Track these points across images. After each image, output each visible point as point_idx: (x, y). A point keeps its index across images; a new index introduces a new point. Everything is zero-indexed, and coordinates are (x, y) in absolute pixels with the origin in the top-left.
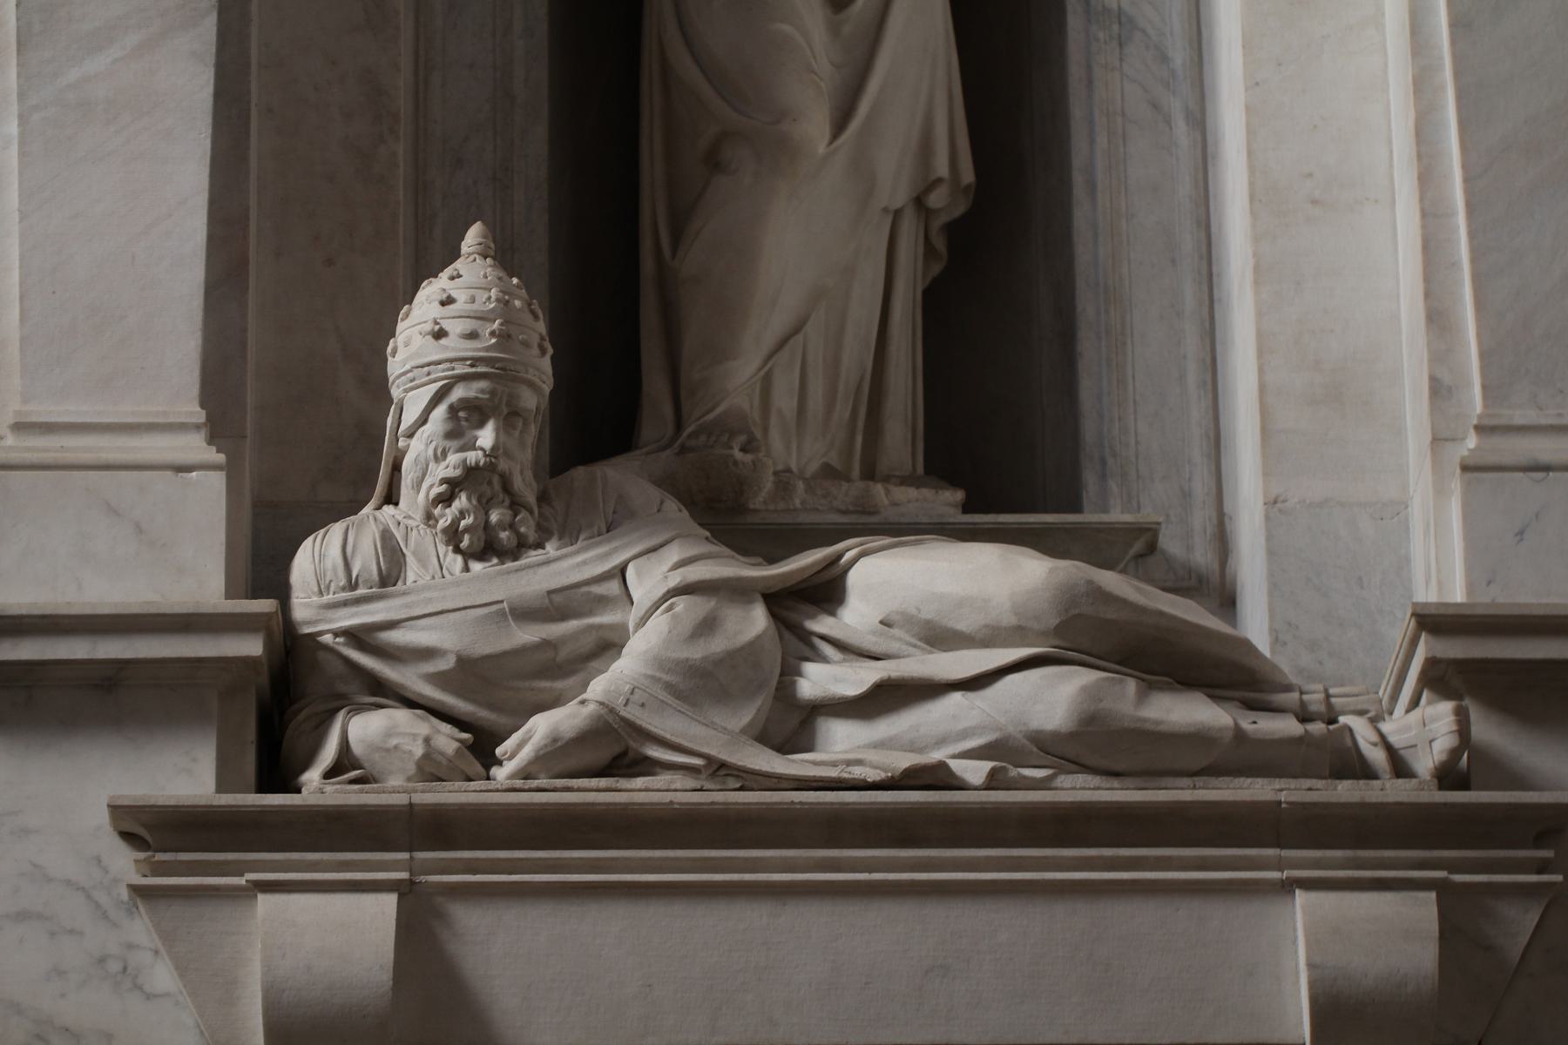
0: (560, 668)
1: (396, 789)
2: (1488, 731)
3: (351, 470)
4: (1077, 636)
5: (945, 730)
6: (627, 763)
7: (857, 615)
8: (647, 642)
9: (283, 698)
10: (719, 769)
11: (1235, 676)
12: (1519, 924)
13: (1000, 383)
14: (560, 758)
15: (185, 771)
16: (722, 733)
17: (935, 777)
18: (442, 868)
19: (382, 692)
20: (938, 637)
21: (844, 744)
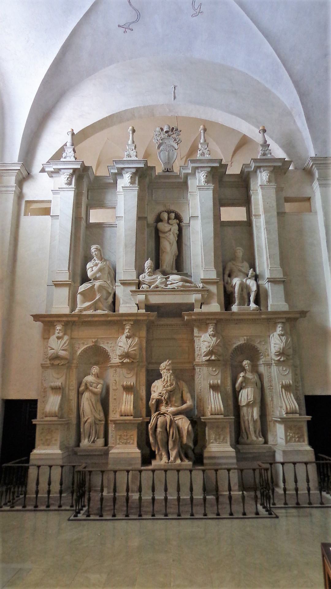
1: (145, 289)
2: (204, 285)
3: (143, 271)
7: (170, 279)
11: (190, 282)
12: (206, 296)
13: (179, 265)
16: (163, 286)
18: (147, 293)
19: (144, 284)
21: (169, 286)
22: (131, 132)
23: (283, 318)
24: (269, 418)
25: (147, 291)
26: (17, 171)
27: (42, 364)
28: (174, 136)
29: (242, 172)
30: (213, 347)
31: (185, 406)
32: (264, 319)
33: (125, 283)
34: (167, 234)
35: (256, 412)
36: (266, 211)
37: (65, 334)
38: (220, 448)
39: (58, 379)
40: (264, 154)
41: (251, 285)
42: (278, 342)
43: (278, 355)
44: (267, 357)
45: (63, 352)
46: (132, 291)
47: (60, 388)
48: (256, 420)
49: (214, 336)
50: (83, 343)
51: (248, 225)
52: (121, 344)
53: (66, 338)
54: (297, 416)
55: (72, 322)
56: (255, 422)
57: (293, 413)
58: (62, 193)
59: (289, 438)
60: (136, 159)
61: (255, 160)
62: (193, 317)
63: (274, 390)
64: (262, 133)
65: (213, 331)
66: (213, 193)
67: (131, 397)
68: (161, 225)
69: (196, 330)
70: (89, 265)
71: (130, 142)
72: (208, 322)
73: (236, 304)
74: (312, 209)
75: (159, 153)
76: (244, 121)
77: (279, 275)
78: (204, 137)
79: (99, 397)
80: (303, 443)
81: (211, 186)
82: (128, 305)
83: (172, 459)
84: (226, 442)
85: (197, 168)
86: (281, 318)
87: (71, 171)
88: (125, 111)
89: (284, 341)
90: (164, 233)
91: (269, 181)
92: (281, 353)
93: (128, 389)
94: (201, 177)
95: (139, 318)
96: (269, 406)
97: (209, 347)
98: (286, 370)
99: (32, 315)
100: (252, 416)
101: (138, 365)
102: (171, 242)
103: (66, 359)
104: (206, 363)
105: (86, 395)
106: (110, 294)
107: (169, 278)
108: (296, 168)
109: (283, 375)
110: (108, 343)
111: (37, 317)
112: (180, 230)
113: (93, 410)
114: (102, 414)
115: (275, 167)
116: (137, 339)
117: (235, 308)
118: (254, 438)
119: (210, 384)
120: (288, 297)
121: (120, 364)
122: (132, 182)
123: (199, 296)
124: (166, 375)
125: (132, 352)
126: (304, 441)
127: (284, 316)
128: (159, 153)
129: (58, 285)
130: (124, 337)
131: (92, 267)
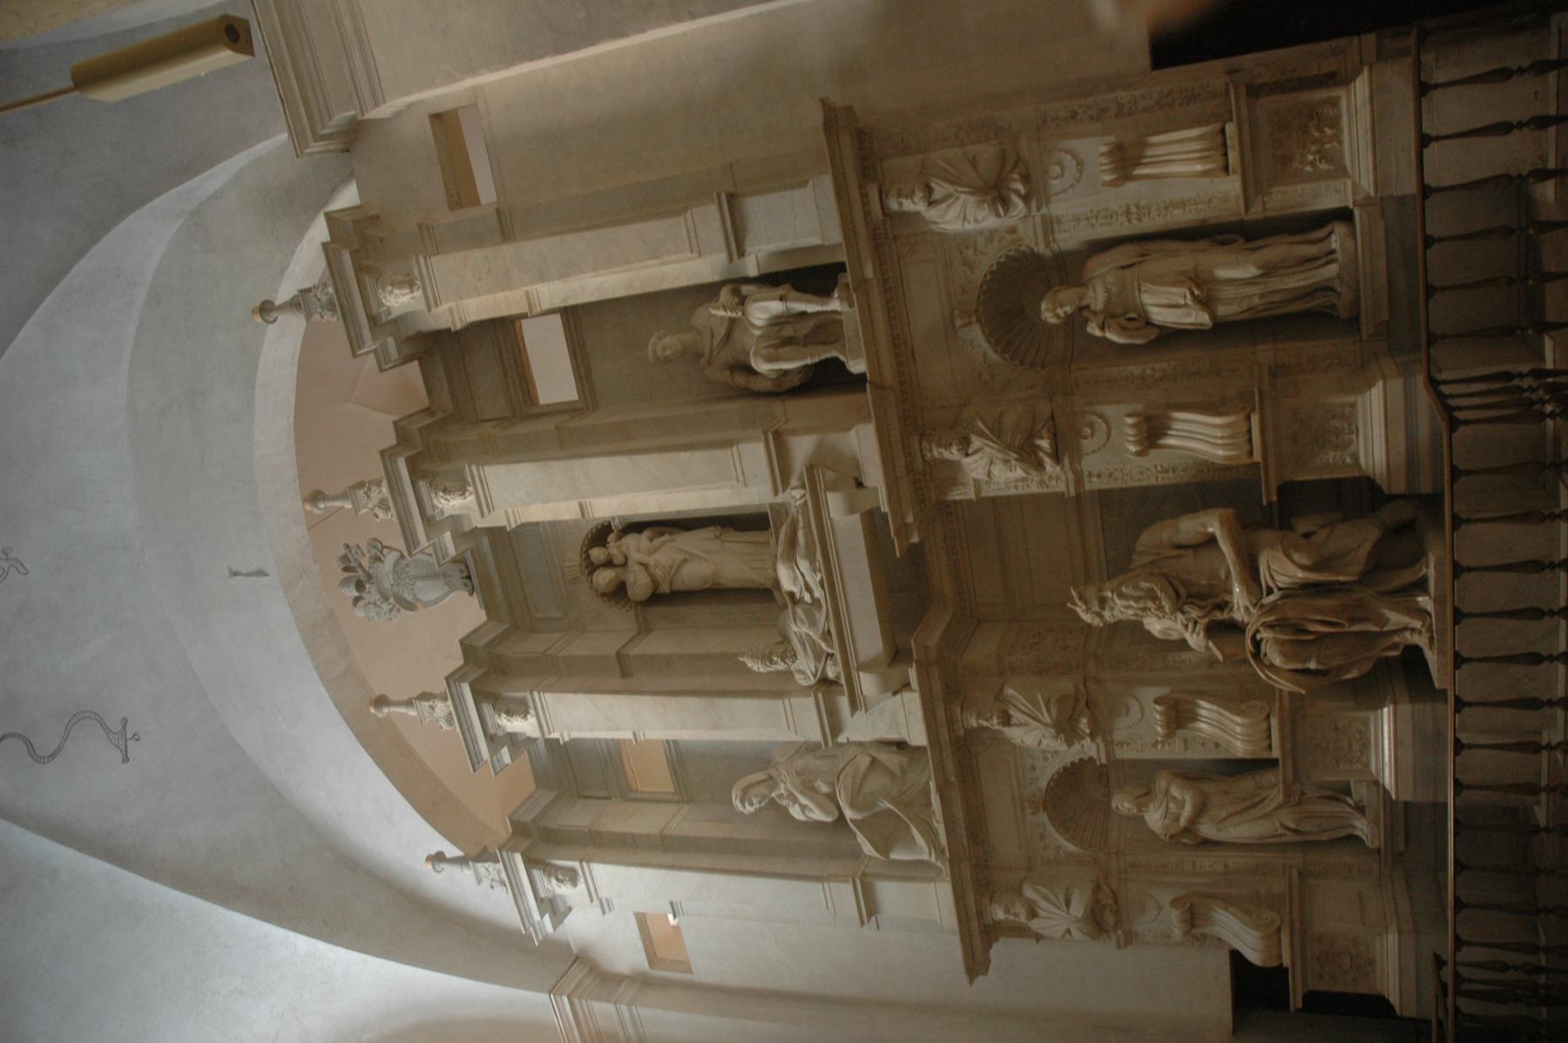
0: (814, 644)
1: (840, 668)
2: (794, 482)
4: (790, 557)
5: (813, 580)
6: (829, 632)
7: (795, 590)
8: (804, 630)
9: (824, 682)
10: (827, 618)
12: (830, 475)
14: (830, 645)
15: (843, 702)
16: (821, 618)
17: (821, 583)
18: (853, 664)
20: (796, 578)
21: (818, 593)
22: (386, 710)
23: (864, 196)
24: (1256, 212)
25: (846, 664)
26: (576, 1001)
27: (1119, 946)
28: (365, 563)
29: (407, 359)
30: (1009, 447)
31: (1225, 547)
32: (880, 262)
33: (834, 725)
34: (659, 573)
35: (1236, 271)
36: (506, 284)
37: (1018, 890)
38: (1375, 427)
39: (1160, 908)
40: (331, 306)
41: (766, 316)
42: (952, 214)
43: (1005, 202)
44: (1021, 232)
45: (1074, 904)
46: (854, 706)
47: (1192, 910)
48: (1259, 267)
49: (965, 443)
50: (1042, 837)
51: (572, 316)
52: (1034, 738)
53: (1029, 892)
54: (1230, 128)
55: (979, 879)
56: (1269, 271)
57: (1225, 144)
58: (603, 894)
59: (1324, 166)
60: (449, 702)
61: (355, 343)
62: (910, 519)
63: (1143, 203)
64: (274, 315)
65: (948, 446)
66: (489, 463)
67: (1206, 709)
68: (639, 585)
69: (956, 495)
70: (795, 812)
71: (412, 713)
72: (919, 465)
73: (843, 358)
74: (465, 103)
75: (426, 604)
76: (261, 363)
77: (710, 218)
78: (337, 498)
79: (1207, 787)
80: (1343, 104)
81: (471, 471)
82: (902, 720)
83: (1417, 624)
84: (1353, 405)
85: (428, 521)
86: (866, 204)
87: (537, 874)
88: (338, 705)
89: (949, 188)
90: (655, 583)
91: (411, 285)
92: (996, 194)
93: (1179, 716)
94: (450, 504)
95: (938, 690)
96: (1202, 216)
97: (1006, 462)
98: (1060, 163)
99: (971, 982)
100: (1250, 282)
101: (1098, 681)
102: (680, 557)
103: (1098, 887)
104: (1066, 461)
105: (1207, 830)
106: (874, 761)
107: (792, 594)
108: (351, 175)
109: (1081, 172)
110: (1033, 769)
111: (976, 965)
112: (635, 527)
113: (1255, 813)
114: (1269, 777)
115: (360, 269)
116: (1009, 691)
117: (857, 366)
118: (1333, 269)
119: (1139, 454)
120: (782, 176)
121: (1099, 740)
122: (521, 709)
123: (835, 503)
124: (1121, 609)
125: (1054, 712)
126: (1335, 103)
127: (855, 195)
128: (426, 604)
129: (870, 907)
130: (1006, 729)
131: (803, 808)
